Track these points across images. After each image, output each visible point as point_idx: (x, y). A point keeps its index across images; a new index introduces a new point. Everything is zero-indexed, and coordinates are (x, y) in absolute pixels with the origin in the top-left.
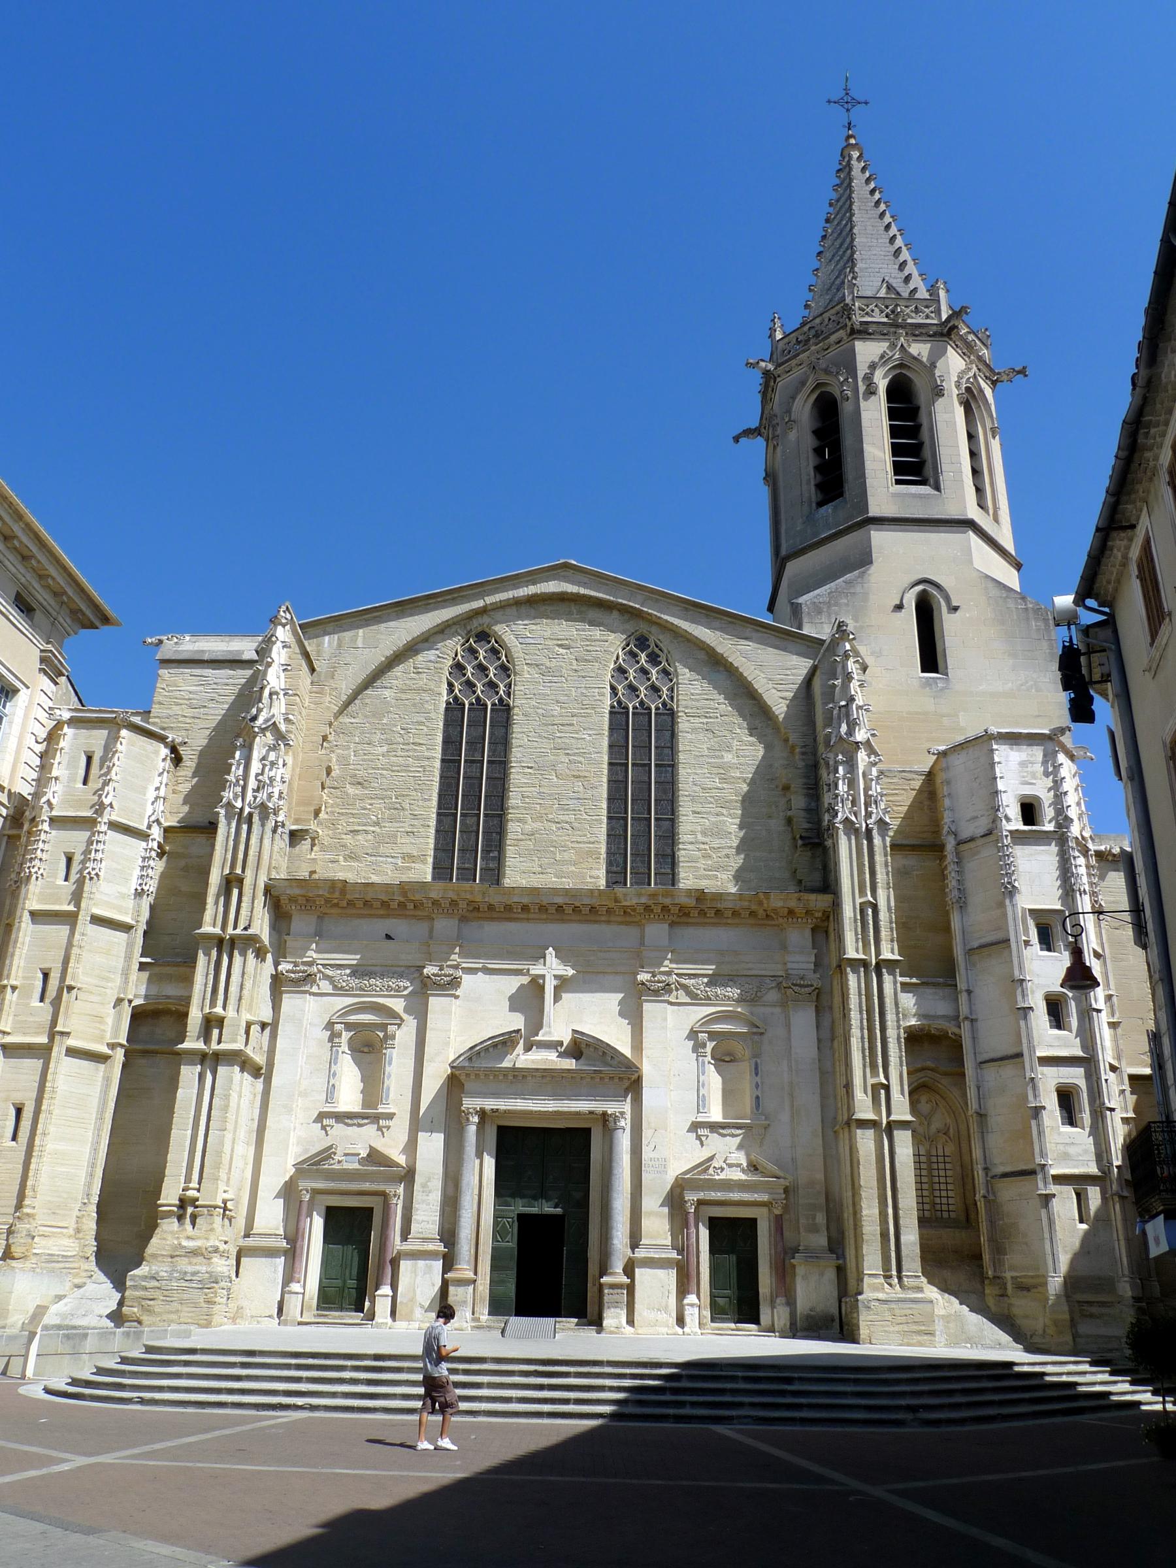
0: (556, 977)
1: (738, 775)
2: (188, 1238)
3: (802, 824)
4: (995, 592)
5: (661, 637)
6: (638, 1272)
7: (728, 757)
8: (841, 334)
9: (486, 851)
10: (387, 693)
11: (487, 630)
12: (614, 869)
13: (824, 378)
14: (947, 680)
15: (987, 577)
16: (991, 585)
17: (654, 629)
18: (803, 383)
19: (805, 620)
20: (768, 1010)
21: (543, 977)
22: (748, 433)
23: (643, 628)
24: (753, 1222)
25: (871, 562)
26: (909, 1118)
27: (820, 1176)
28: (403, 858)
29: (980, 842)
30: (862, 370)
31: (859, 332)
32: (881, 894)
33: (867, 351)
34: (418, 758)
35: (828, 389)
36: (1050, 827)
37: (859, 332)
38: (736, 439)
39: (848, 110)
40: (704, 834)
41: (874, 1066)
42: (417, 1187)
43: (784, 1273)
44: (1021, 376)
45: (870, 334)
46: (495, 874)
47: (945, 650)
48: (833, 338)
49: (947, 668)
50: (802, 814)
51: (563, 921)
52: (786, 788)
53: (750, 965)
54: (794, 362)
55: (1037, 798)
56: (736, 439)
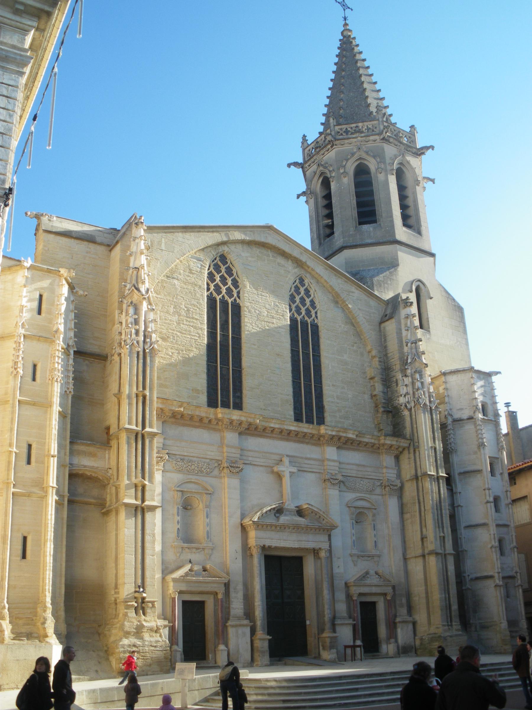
0: (290, 472)
1: (349, 367)
2: (145, 620)
3: (381, 398)
4: (444, 294)
5: (312, 281)
6: (338, 628)
7: (346, 357)
8: (377, 137)
9: (234, 392)
10: (176, 282)
11: (226, 255)
12: (297, 411)
13: (364, 156)
14: (430, 334)
15: (441, 285)
16: (443, 290)
17: (308, 275)
18: (353, 154)
19: (375, 288)
20: (377, 497)
21: (284, 471)
22: (296, 164)
23: (302, 272)
24: (374, 604)
25: (398, 265)
26: (453, 552)
27: (403, 580)
28: (192, 390)
29: (466, 421)
30: (388, 161)
31: (386, 140)
32: (437, 442)
33: (390, 150)
34: (195, 328)
35: (366, 162)
36: (492, 418)
37: (386, 140)
38: (289, 165)
39: (344, 10)
40: (338, 397)
41: (439, 527)
42: (231, 590)
43: (392, 626)
44: (431, 183)
45: (390, 142)
46: (238, 406)
47: (428, 318)
48: (372, 138)
49: (429, 328)
50: (381, 394)
51: (287, 440)
52: (372, 378)
53: (369, 473)
54: (346, 141)
55: (486, 403)
56: (289, 165)
